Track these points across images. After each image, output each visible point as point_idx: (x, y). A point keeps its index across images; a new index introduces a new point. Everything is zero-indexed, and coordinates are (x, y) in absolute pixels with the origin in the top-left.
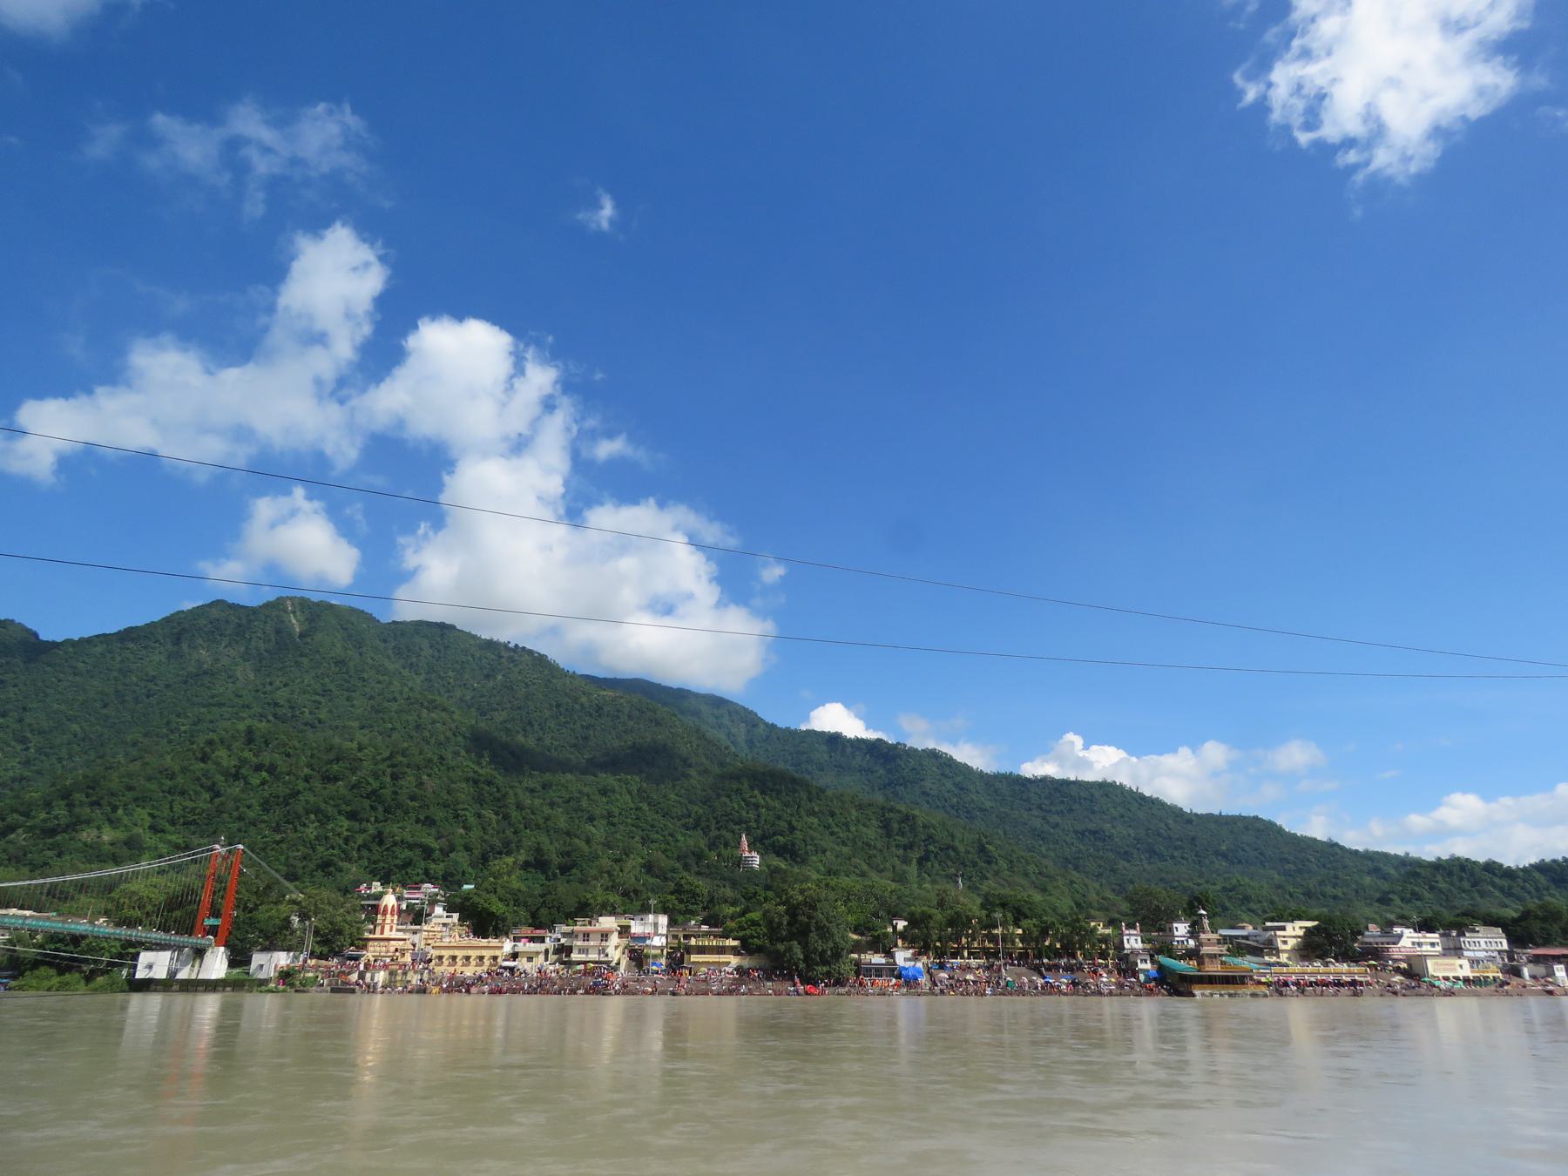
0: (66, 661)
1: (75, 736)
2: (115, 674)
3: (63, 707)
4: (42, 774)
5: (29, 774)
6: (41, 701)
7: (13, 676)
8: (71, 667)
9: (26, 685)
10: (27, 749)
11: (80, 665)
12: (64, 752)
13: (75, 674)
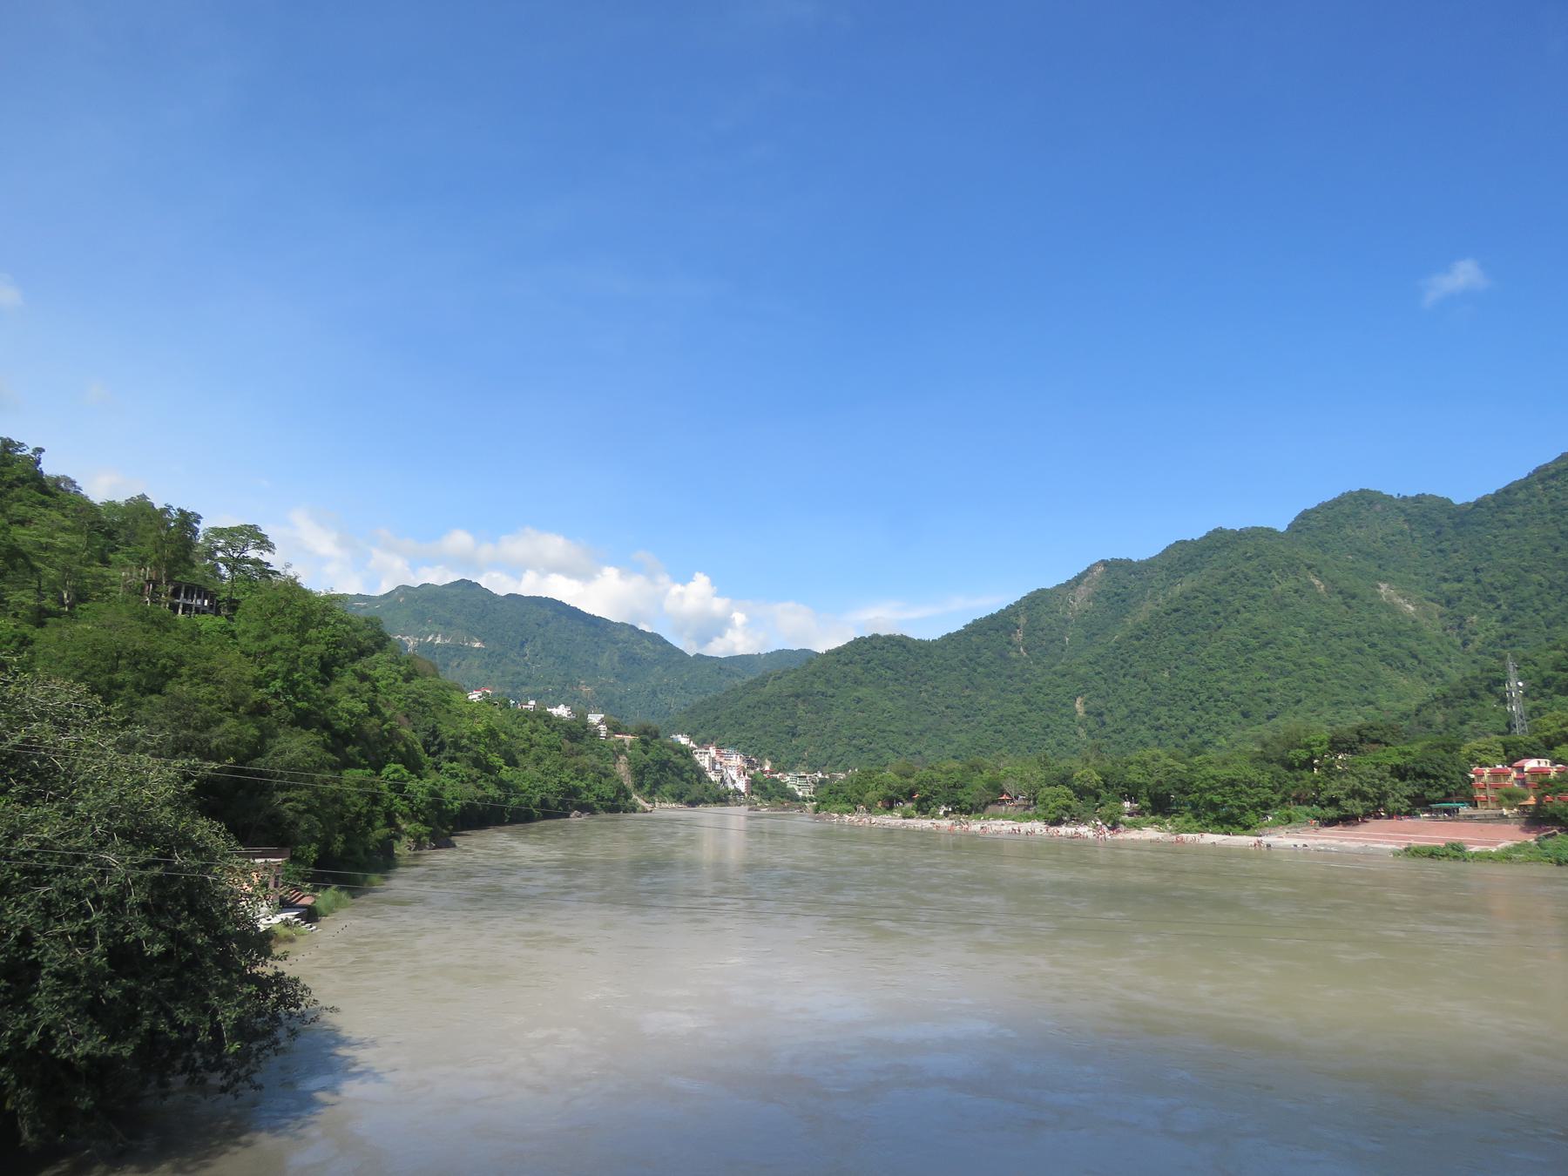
0: (1493, 516)
1: (1540, 585)
2: (1550, 516)
3: (1513, 560)
4: (1526, 628)
5: (1514, 630)
6: (1488, 560)
7: (1449, 543)
8: (1500, 521)
9: (1465, 548)
10: (1499, 607)
11: (1509, 517)
12: (1538, 604)
13: (1508, 527)
